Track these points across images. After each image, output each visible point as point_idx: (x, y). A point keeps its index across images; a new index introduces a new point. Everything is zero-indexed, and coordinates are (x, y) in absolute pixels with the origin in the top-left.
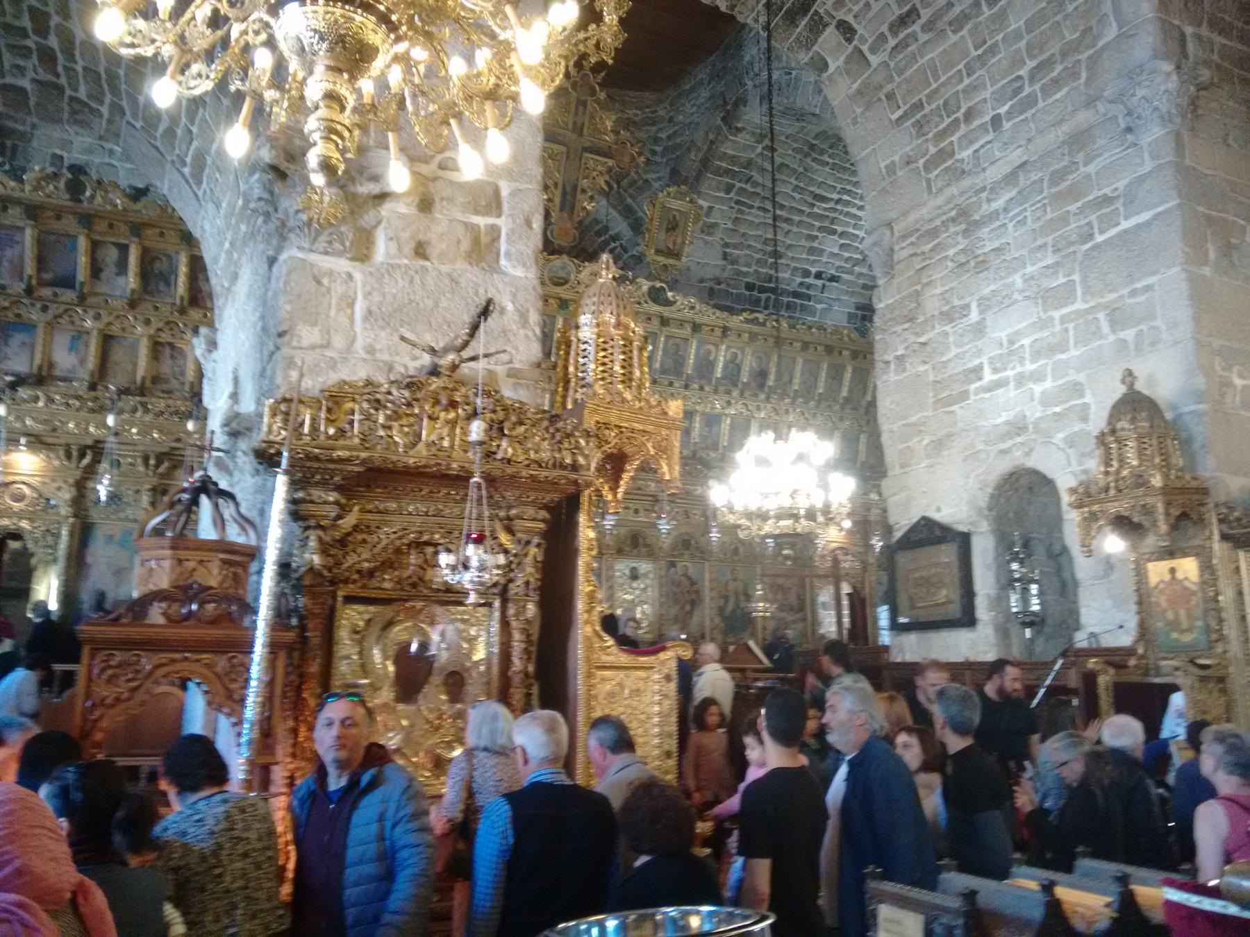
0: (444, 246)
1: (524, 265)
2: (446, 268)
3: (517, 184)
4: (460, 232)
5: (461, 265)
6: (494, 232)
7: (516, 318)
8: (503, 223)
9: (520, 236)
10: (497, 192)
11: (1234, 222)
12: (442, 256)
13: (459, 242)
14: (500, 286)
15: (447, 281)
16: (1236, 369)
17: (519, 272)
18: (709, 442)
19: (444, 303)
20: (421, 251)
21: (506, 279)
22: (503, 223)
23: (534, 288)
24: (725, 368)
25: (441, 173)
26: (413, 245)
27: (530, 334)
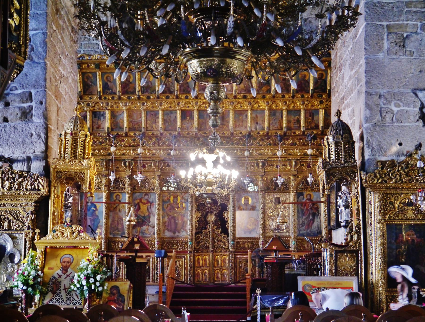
0: (12, 117)
1: (39, 118)
2: (12, 125)
3: (37, 90)
4: (17, 110)
5: (18, 122)
6: (31, 108)
7: (36, 137)
8: (33, 104)
9: (38, 108)
10: (30, 94)
11: (407, 24)
12: (11, 120)
13: (17, 114)
14: (31, 127)
15: (13, 129)
16: (393, 103)
17: (38, 121)
18: (313, 125)
19: (12, 136)
20: (6, 120)
21: (33, 124)
22: (33, 104)
23: (43, 125)
24: (316, 83)
25: (11, 92)
26: (2, 118)
27: (41, 142)
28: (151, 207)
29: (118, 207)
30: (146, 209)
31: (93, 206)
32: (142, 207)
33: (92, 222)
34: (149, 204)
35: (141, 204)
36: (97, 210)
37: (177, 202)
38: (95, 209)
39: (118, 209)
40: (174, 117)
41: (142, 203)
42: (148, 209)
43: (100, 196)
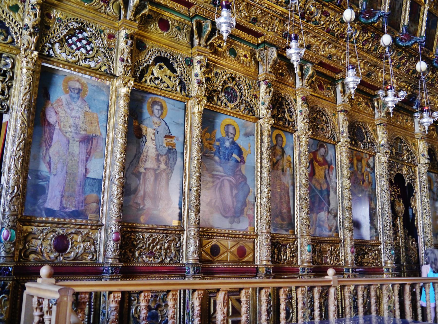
28: (330, 173)
29: (280, 164)
30: (323, 176)
31: (236, 151)
32: (316, 171)
33: (235, 192)
34: (327, 167)
35: (316, 164)
36: (243, 161)
37: (361, 171)
38: (239, 159)
39: (280, 168)
40: (399, 5)
41: (317, 161)
42: (325, 177)
43: (249, 130)
